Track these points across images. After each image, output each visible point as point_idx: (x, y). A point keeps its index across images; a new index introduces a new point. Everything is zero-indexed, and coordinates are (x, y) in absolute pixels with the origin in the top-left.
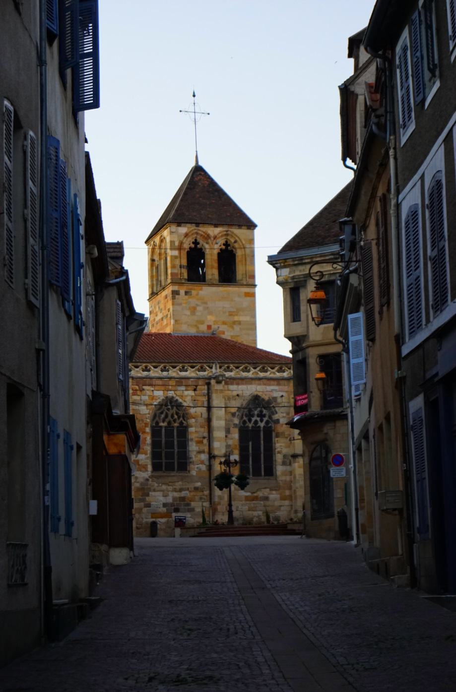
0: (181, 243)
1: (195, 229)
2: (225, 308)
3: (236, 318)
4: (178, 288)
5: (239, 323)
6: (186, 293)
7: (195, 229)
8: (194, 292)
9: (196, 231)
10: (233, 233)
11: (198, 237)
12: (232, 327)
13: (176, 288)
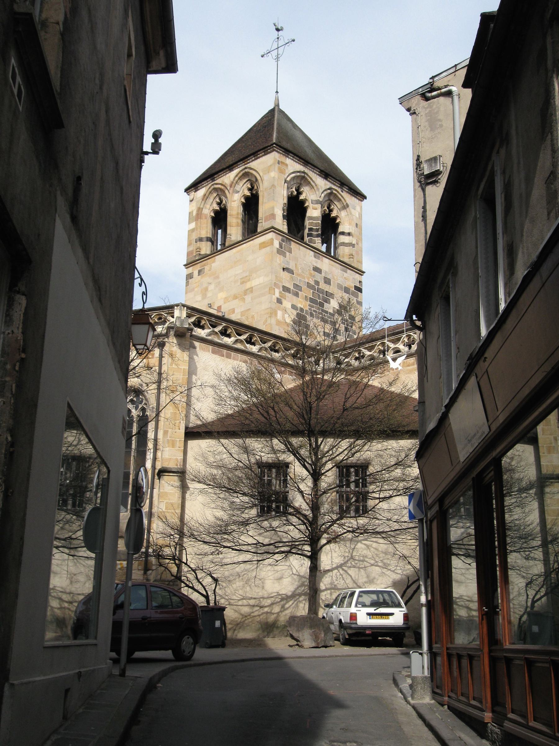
0: (200, 210)
1: (213, 185)
2: (237, 274)
3: (248, 285)
4: (193, 270)
5: (251, 290)
6: (200, 272)
7: (213, 185)
8: (207, 268)
9: (213, 187)
10: (251, 169)
11: (220, 193)
12: (243, 300)
13: (190, 270)
